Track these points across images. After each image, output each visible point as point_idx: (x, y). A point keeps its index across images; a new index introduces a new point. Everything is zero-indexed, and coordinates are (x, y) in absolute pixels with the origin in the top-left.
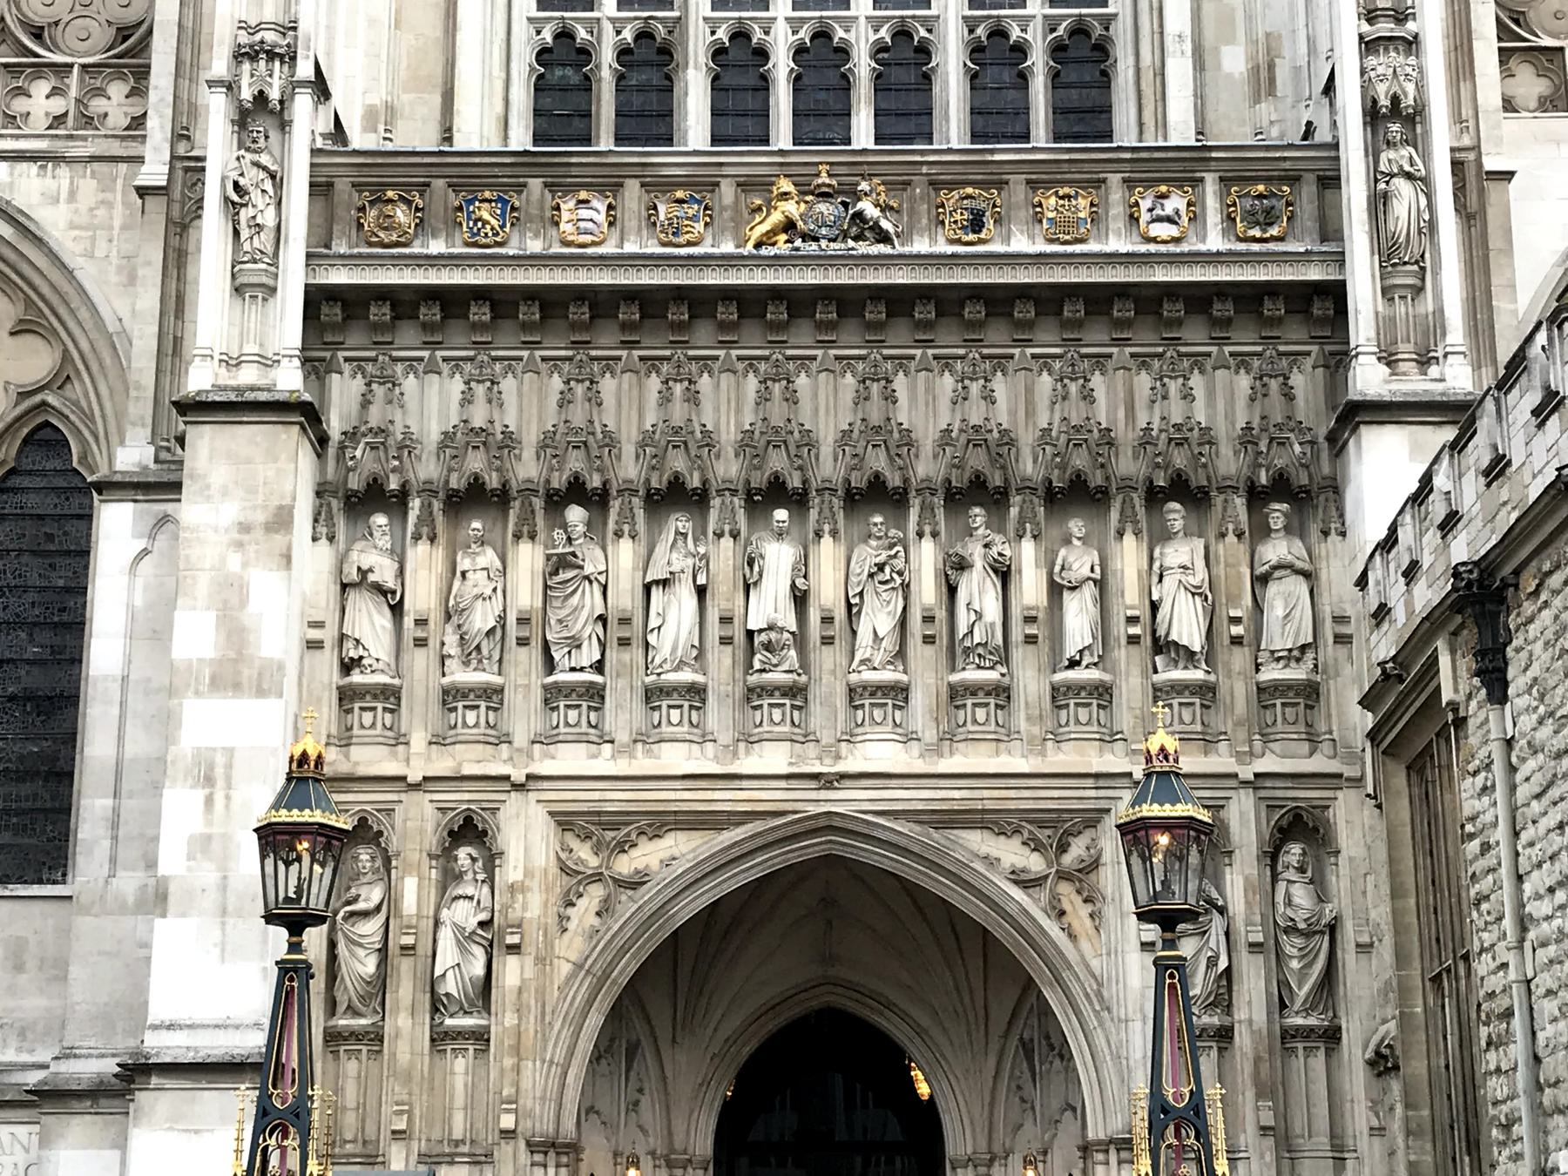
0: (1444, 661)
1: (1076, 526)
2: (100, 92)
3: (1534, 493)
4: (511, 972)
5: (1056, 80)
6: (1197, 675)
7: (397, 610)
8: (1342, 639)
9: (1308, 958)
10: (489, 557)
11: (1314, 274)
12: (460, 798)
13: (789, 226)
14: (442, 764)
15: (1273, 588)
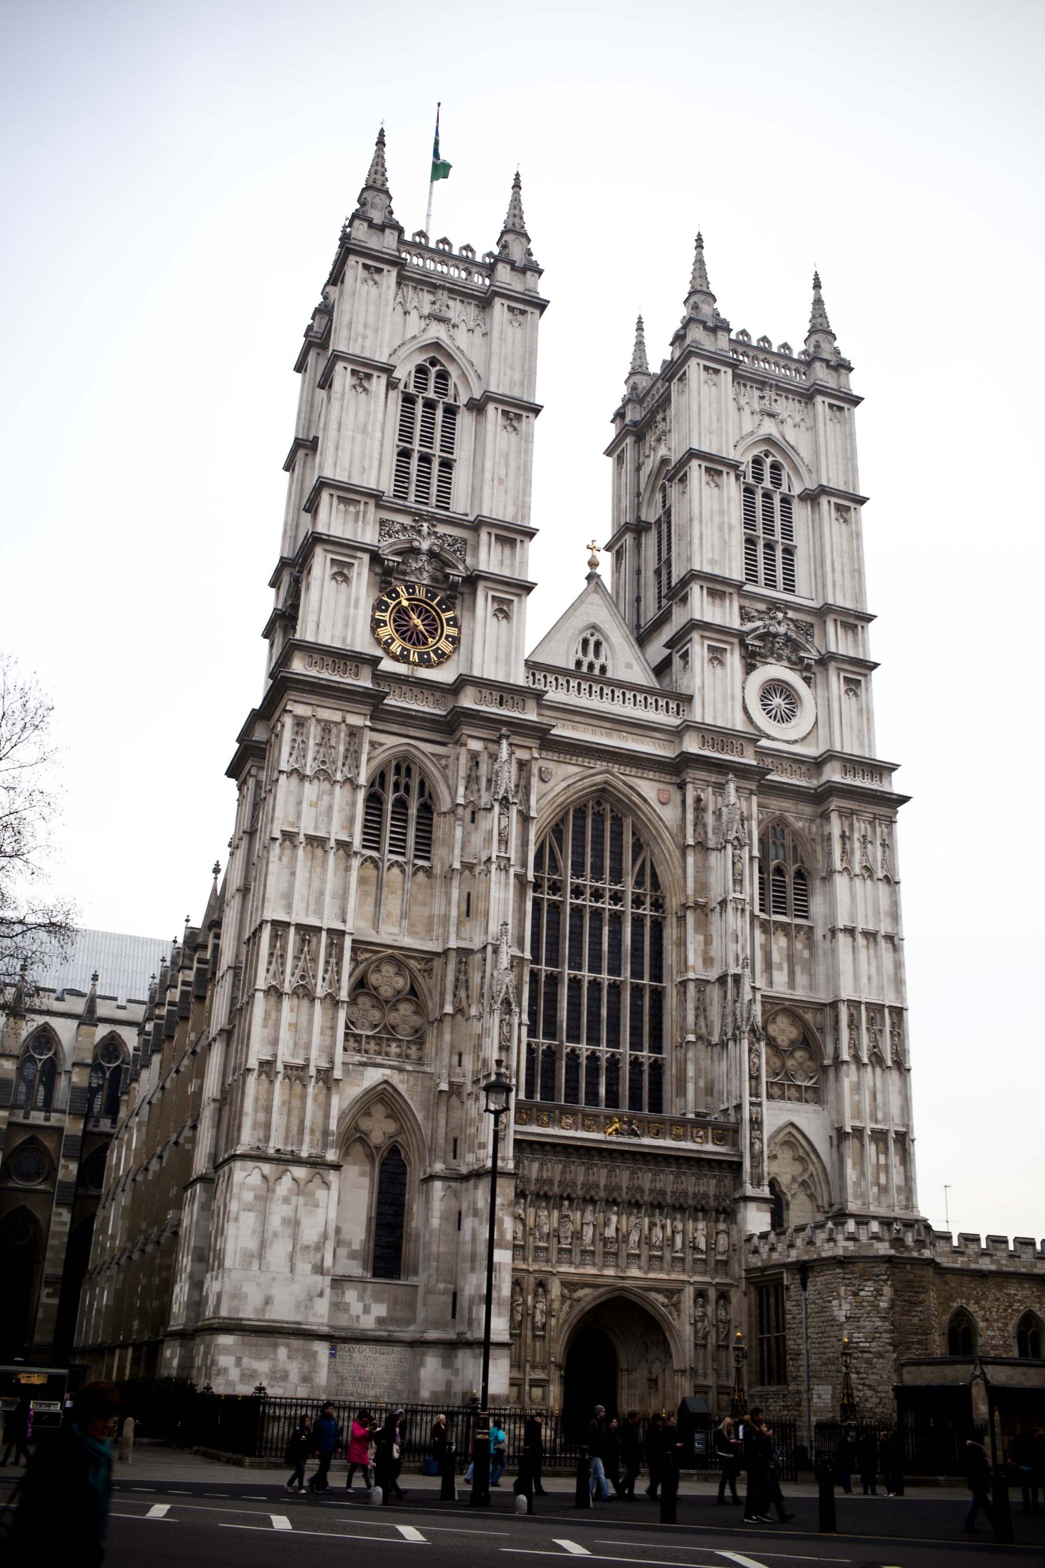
0: (785, 1275)
1: (678, 1216)
2: (410, 1048)
3: (824, 1255)
4: (553, 1321)
5: (650, 1075)
6: (704, 1257)
7: (524, 1225)
8: (734, 1250)
9: (724, 1328)
10: (546, 1213)
11: (735, 1159)
12: (540, 1276)
13: (616, 1130)
14: (536, 1267)
15: (720, 1236)
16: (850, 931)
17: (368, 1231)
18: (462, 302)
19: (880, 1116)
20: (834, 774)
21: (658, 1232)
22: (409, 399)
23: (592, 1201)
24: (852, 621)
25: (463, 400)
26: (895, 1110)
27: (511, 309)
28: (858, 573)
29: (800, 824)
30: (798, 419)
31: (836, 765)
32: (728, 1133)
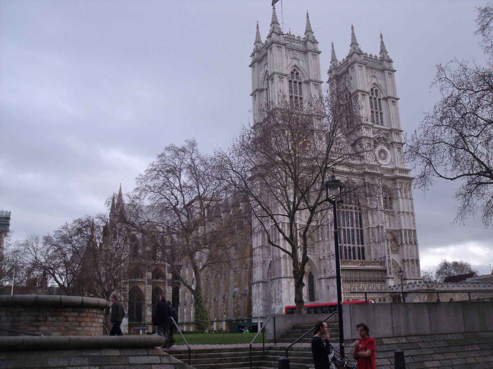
3: (411, 290)
16: (403, 212)
17: (307, 292)
18: (300, 53)
19: (412, 256)
20: (398, 174)
21: (370, 287)
22: (290, 81)
23: (357, 281)
24: (398, 132)
25: (303, 80)
26: (415, 255)
27: (312, 54)
28: (398, 119)
29: (389, 186)
30: (381, 76)
31: (398, 171)
32: (382, 263)
